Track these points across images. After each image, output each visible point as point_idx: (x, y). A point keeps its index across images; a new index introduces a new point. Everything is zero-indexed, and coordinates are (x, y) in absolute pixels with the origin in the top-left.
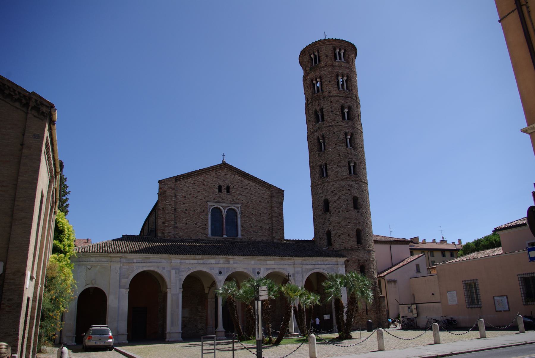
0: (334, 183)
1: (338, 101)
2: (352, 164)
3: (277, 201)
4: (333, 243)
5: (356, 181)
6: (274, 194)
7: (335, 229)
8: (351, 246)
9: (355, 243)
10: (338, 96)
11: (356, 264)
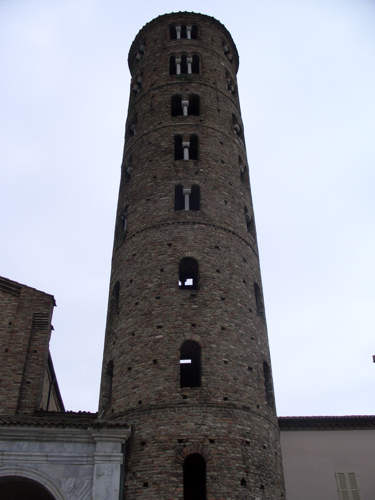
0: (134, 239)
1: (166, 91)
2: (187, 190)
3: (31, 318)
4: (114, 395)
5: (194, 223)
6: (26, 304)
7: (122, 353)
8: (160, 394)
9: (175, 384)
10: (167, 85)
11: (171, 452)
